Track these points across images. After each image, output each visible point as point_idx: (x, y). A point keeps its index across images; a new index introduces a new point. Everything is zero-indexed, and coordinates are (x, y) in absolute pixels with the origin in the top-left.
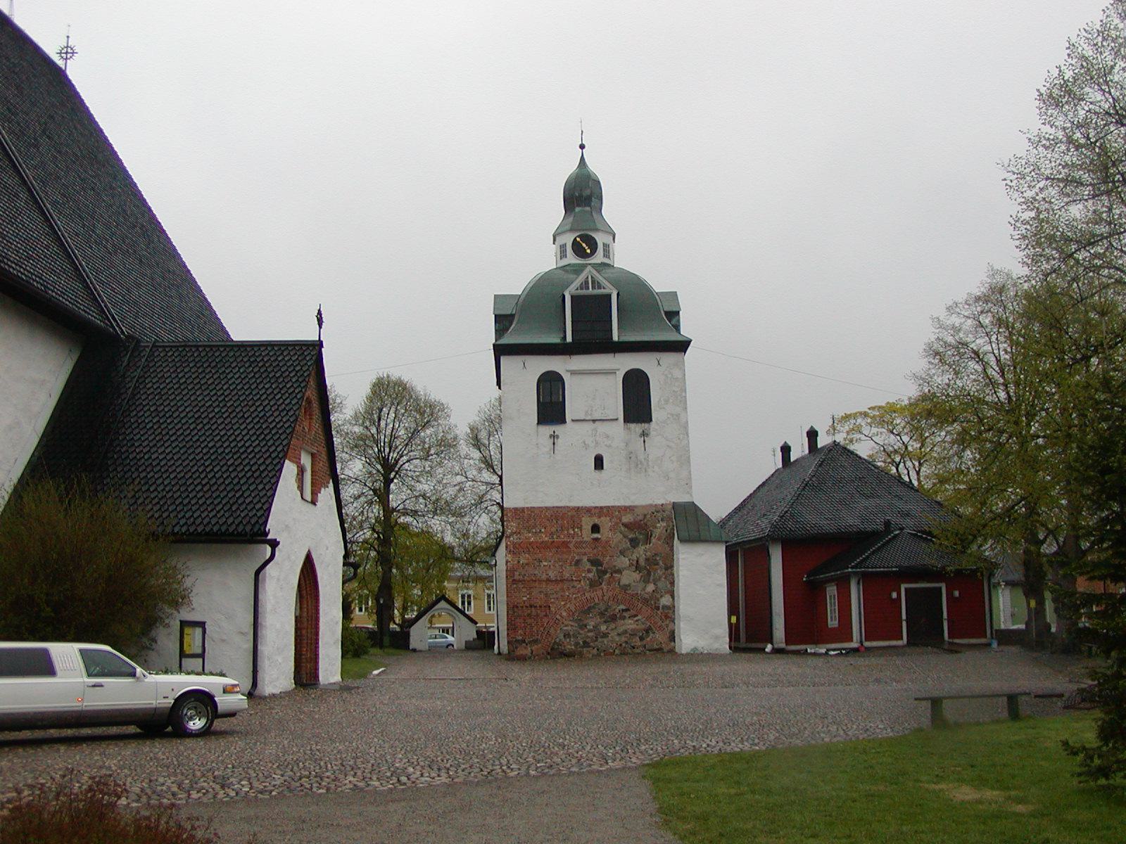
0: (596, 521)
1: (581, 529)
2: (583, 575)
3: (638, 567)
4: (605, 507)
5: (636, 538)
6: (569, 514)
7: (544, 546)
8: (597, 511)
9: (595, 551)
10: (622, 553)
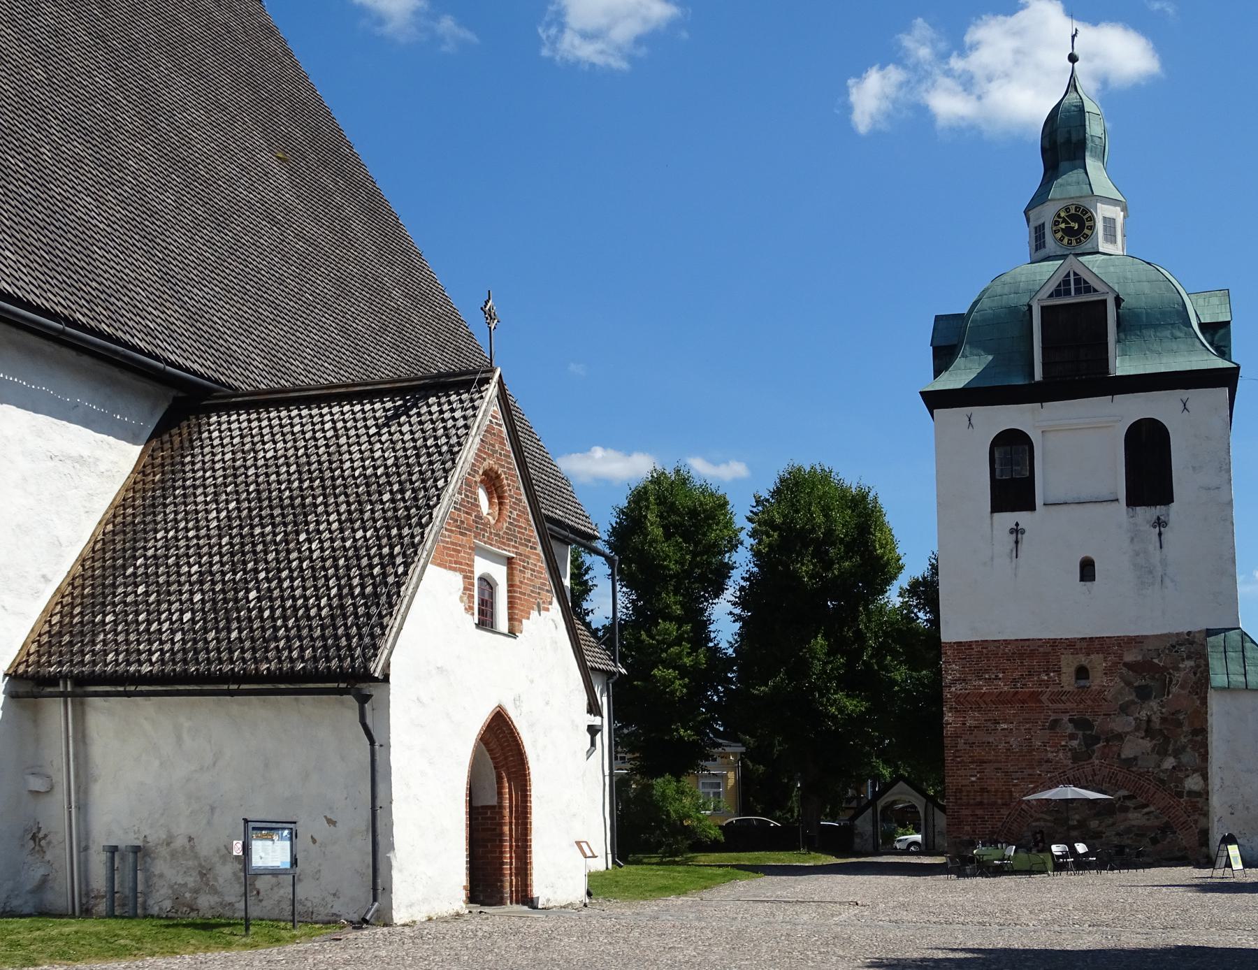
0: (1083, 660)
1: (1059, 672)
2: (1063, 743)
3: (1149, 732)
4: (1097, 638)
5: (1146, 686)
6: (1041, 650)
7: (1002, 699)
8: (1084, 645)
9: (1082, 706)
10: (1124, 709)
